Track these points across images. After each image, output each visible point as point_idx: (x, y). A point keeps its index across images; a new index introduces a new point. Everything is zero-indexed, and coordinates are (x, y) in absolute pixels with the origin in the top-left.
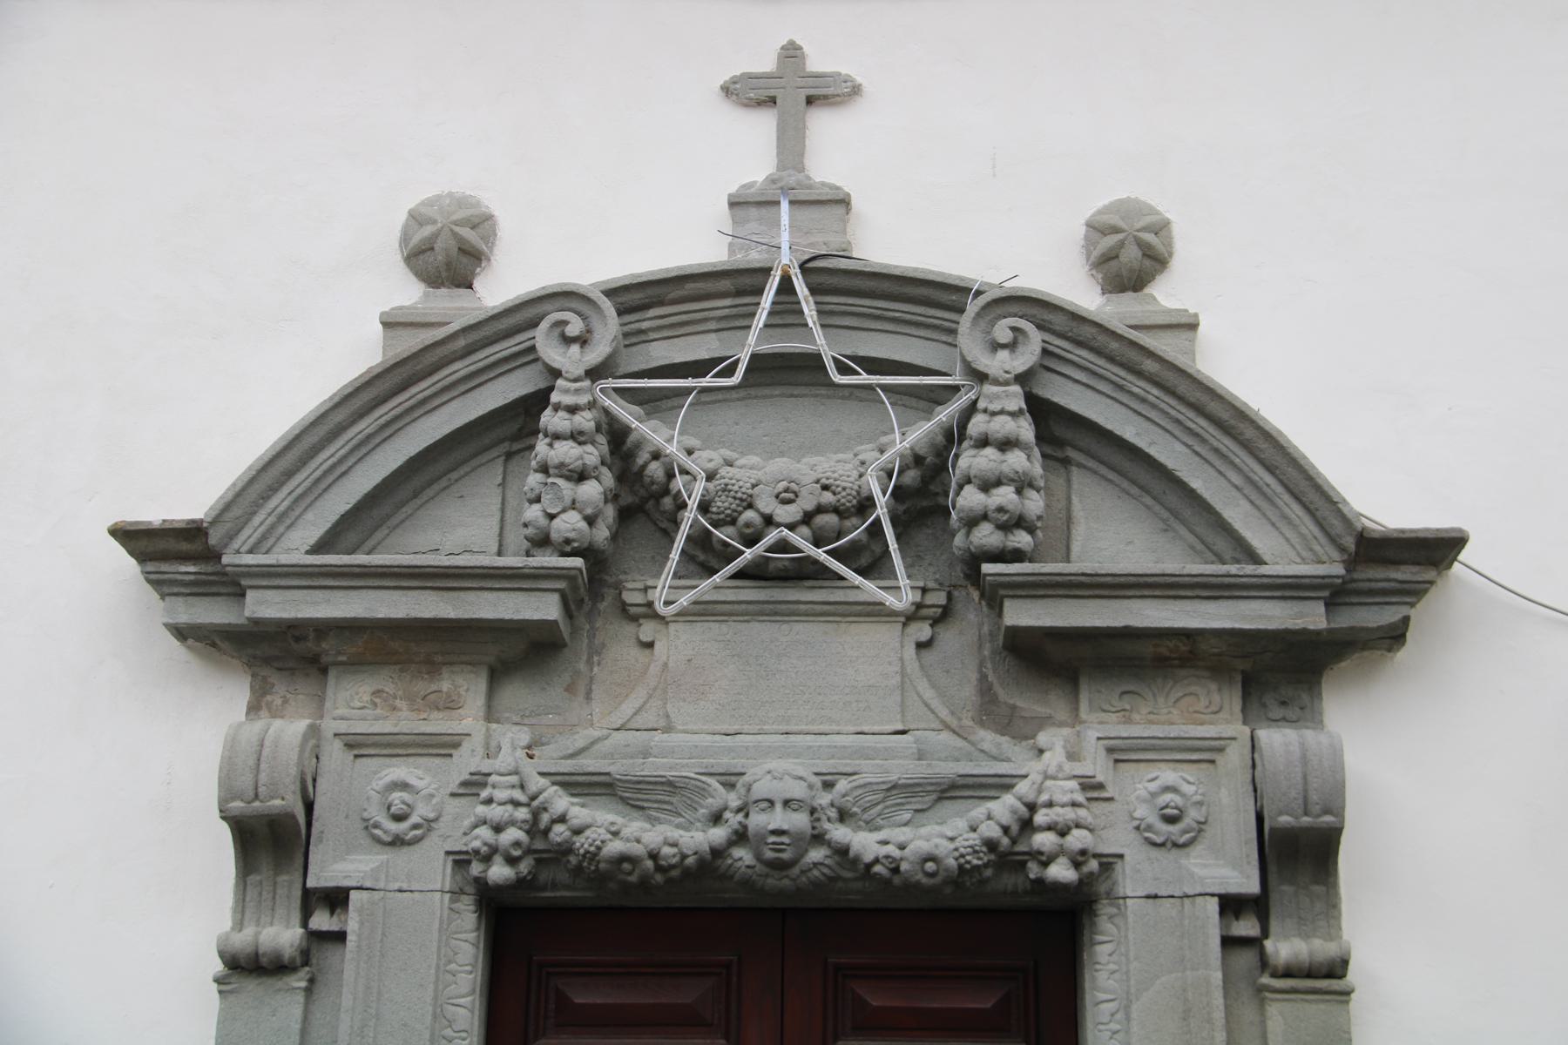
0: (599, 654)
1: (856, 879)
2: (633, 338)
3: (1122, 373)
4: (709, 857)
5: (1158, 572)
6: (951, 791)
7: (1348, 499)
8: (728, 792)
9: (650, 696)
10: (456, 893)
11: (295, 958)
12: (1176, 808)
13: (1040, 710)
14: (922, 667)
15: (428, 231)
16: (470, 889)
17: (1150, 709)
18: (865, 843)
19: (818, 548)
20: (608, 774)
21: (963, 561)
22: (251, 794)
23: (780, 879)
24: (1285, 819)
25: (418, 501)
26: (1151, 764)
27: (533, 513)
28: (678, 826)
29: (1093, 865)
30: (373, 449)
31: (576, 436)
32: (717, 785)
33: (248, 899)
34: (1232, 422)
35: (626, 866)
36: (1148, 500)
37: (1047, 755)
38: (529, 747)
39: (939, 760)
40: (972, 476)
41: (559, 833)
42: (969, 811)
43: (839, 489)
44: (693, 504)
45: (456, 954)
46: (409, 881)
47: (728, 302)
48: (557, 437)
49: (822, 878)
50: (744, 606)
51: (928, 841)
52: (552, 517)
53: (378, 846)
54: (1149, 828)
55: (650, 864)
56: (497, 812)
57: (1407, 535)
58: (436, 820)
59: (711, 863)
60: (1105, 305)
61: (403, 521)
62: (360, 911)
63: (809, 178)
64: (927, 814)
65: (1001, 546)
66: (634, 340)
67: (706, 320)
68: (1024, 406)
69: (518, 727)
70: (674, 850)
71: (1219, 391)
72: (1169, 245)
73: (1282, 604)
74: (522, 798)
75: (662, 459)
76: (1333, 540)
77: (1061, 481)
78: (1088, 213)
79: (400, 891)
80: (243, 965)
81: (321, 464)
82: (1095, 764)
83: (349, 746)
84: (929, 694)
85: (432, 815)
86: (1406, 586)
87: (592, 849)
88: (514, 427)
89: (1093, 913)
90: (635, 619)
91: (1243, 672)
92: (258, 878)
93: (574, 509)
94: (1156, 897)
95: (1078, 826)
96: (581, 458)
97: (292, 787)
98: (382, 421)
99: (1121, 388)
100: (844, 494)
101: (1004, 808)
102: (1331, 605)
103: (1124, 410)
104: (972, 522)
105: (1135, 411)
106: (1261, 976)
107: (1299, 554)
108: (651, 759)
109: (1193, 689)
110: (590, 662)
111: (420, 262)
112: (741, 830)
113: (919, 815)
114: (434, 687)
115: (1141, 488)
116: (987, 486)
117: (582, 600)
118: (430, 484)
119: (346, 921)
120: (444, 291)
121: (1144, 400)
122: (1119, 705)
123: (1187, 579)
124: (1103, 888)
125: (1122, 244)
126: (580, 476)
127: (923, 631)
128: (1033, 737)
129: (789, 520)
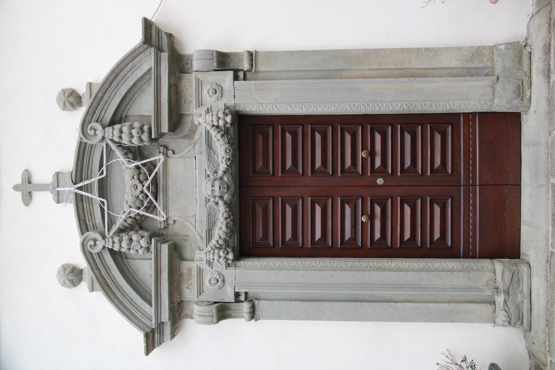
0: (177, 234)
1: (231, 169)
2: (95, 228)
3: (102, 102)
4: (226, 205)
5: (154, 93)
6: (209, 146)
7: (135, 46)
8: (210, 201)
9: (187, 221)
10: (236, 266)
11: (251, 303)
12: (213, 91)
13: (189, 123)
14: (179, 153)
15: (67, 281)
16: (235, 263)
17: (189, 97)
18: (223, 167)
19: (148, 179)
20: (206, 231)
21: (152, 142)
22: (212, 317)
23: (231, 187)
24: (215, 64)
25: (139, 281)
26: (202, 96)
27: (140, 251)
28: (219, 213)
29: (227, 111)
30: (125, 292)
31: (120, 242)
32: (209, 203)
33: (237, 315)
34: (115, 74)
35: (229, 225)
36: (136, 96)
37: (200, 122)
38: (200, 250)
39: (202, 148)
40: (129, 140)
41: (221, 242)
42: (214, 142)
43: (133, 174)
44: (137, 211)
45: (250, 265)
46: (233, 278)
47: (85, 203)
48: (121, 246)
49: (231, 177)
50: (164, 198)
51: (222, 151)
52: (142, 247)
53: (225, 285)
54: (218, 97)
55: (228, 220)
56: (216, 258)
57: (144, 32)
58: (218, 272)
59: (228, 205)
60: (85, 106)
61: (144, 284)
62: (240, 289)
63: (51, 183)
64: (215, 152)
65: (147, 133)
66: (95, 227)
67: (90, 209)
68: (111, 127)
69: (195, 253)
70: (225, 214)
71: (107, 77)
72: (69, 89)
73: (162, 63)
74: (213, 251)
75: (126, 219)
76: (145, 50)
77: (131, 118)
78: (60, 110)
79: (235, 280)
80: (252, 315)
81: (129, 305)
82: (202, 110)
83: (200, 294)
84: (186, 151)
85: (217, 273)
86: (157, 33)
87: (224, 234)
88: (119, 257)
89: (239, 111)
90: (168, 225)
91: (179, 73)
92: (232, 313)
93: (139, 241)
94: (234, 96)
95: (218, 115)
96: (126, 240)
97: (210, 307)
98: (117, 291)
99: (106, 102)
100: (135, 173)
101: (213, 132)
102: (162, 51)
103: (112, 102)
104: (141, 140)
105: (112, 99)
106: (253, 72)
107: (149, 59)
108: (203, 220)
109: (184, 85)
110: (179, 236)
111: (76, 283)
112: (220, 197)
113: (215, 154)
114: (186, 274)
115: (133, 97)
116: (132, 137)
117: (163, 238)
118: (134, 278)
119: (242, 292)
120: (83, 276)
121: (109, 96)
122: (188, 104)
123: (155, 86)
124: (233, 109)
125: (68, 102)
126: (131, 240)
127: (170, 153)
128: (196, 125)
129: (141, 187)
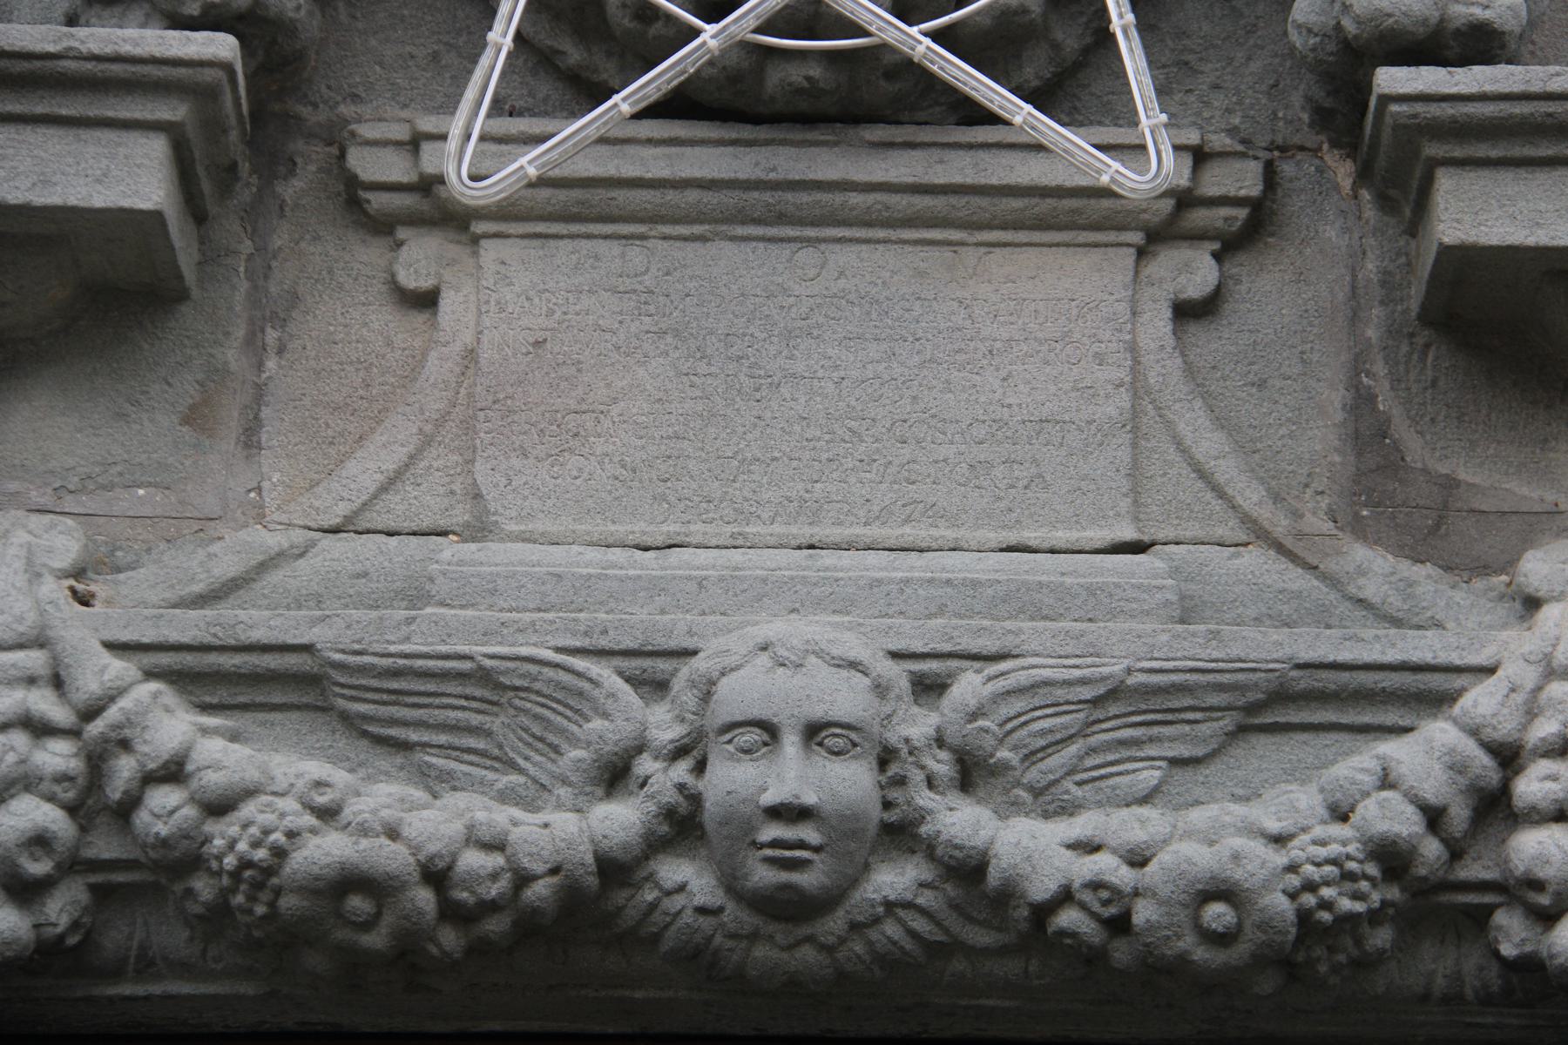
1: (1002, 951)
4: (592, 881)
9: (427, 441)
13: (1526, 492)
14: (1189, 370)
20: (307, 648)
23: (798, 944)
28: (504, 797)
35: (357, 904)
38: (78, 573)
42: (1325, 765)
49: (908, 944)
55: (424, 898)
70: (496, 860)
74: (59, 714)
84: (1209, 444)
87: (261, 854)
90: (383, 227)
108: (429, 610)
110: (254, 345)
112: (684, 807)
113: (1180, 774)
117: (233, 168)
128: (1508, 564)
